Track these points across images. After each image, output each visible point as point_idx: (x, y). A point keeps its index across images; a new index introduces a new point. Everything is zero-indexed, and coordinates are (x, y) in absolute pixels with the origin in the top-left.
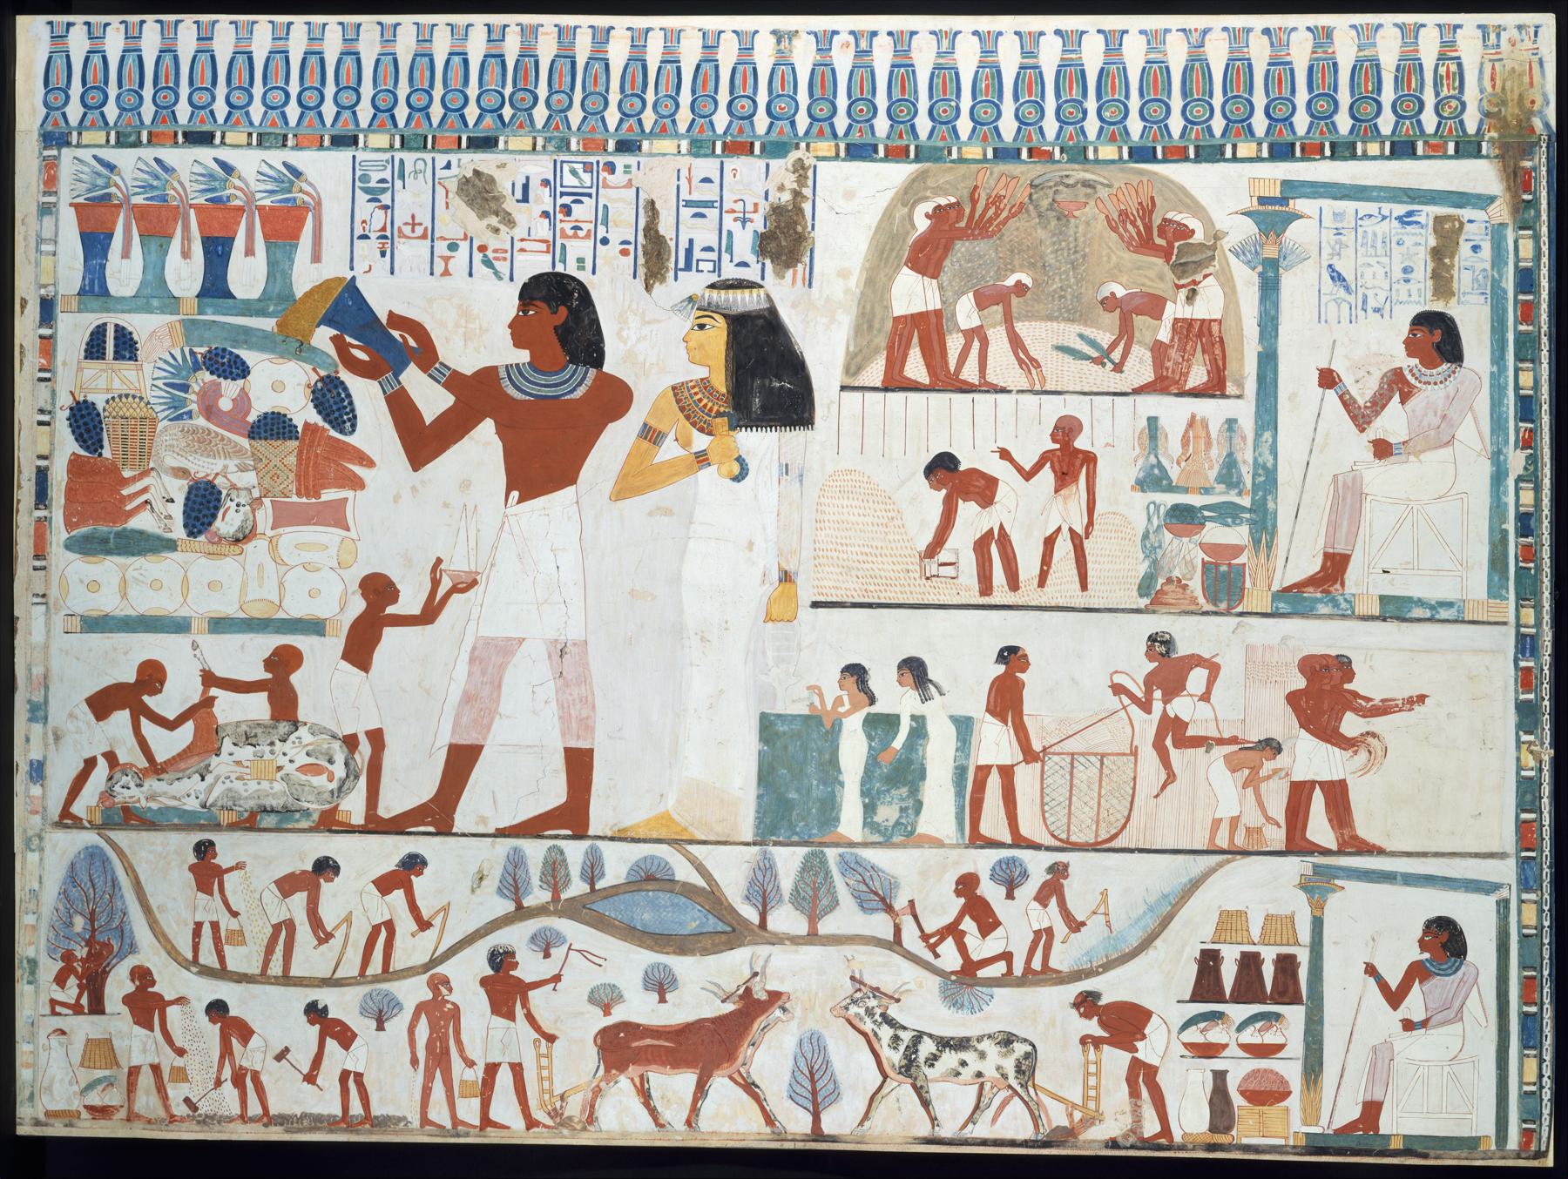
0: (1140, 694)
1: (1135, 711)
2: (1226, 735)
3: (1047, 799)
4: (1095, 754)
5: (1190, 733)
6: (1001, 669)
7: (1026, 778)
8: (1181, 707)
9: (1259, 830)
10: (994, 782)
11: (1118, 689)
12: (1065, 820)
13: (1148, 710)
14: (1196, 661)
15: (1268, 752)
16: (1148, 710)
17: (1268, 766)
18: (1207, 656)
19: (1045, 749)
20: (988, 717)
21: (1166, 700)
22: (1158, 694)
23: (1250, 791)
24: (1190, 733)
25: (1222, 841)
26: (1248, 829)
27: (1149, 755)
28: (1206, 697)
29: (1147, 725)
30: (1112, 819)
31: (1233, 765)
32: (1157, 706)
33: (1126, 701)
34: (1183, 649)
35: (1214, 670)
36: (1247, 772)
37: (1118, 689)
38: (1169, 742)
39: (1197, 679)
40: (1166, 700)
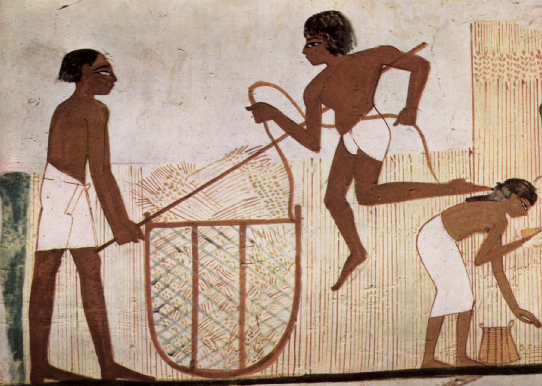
0: (299, 119)
1: (292, 147)
2: (444, 178)
3: (156, 303)
4: (231, 223)
5: (383, 179)
6: (69, 89)
7: (120, 268)
8: (369, 137)
9: (504, 333)
10: (68, 279)
11: (262, 112)
12: (188, 334)
13: (315, 146)
14: (387, 57)
15: (516, 202)
16: (315, 146)
17: (515, 226)
18: (405, 47)
19: (148, 218)
20: (52, 171)
21: (344, 126)
22: (329, 117)
23: (488, 267)
24: (383, 179)
25: (446, 353)
26: (487, 331)
27: (320, 223)
28: (408, 117)
29: (313, 169)
30: (265, 330)
31: (457, 226)
32: (329, 139)
33: (277, 131)
34: (365, 39)
35: (418, 70)
36: (480, 238)
37: (262, 112)
38: (351, 196)
39: (392, 88)
40: (344, 126)
